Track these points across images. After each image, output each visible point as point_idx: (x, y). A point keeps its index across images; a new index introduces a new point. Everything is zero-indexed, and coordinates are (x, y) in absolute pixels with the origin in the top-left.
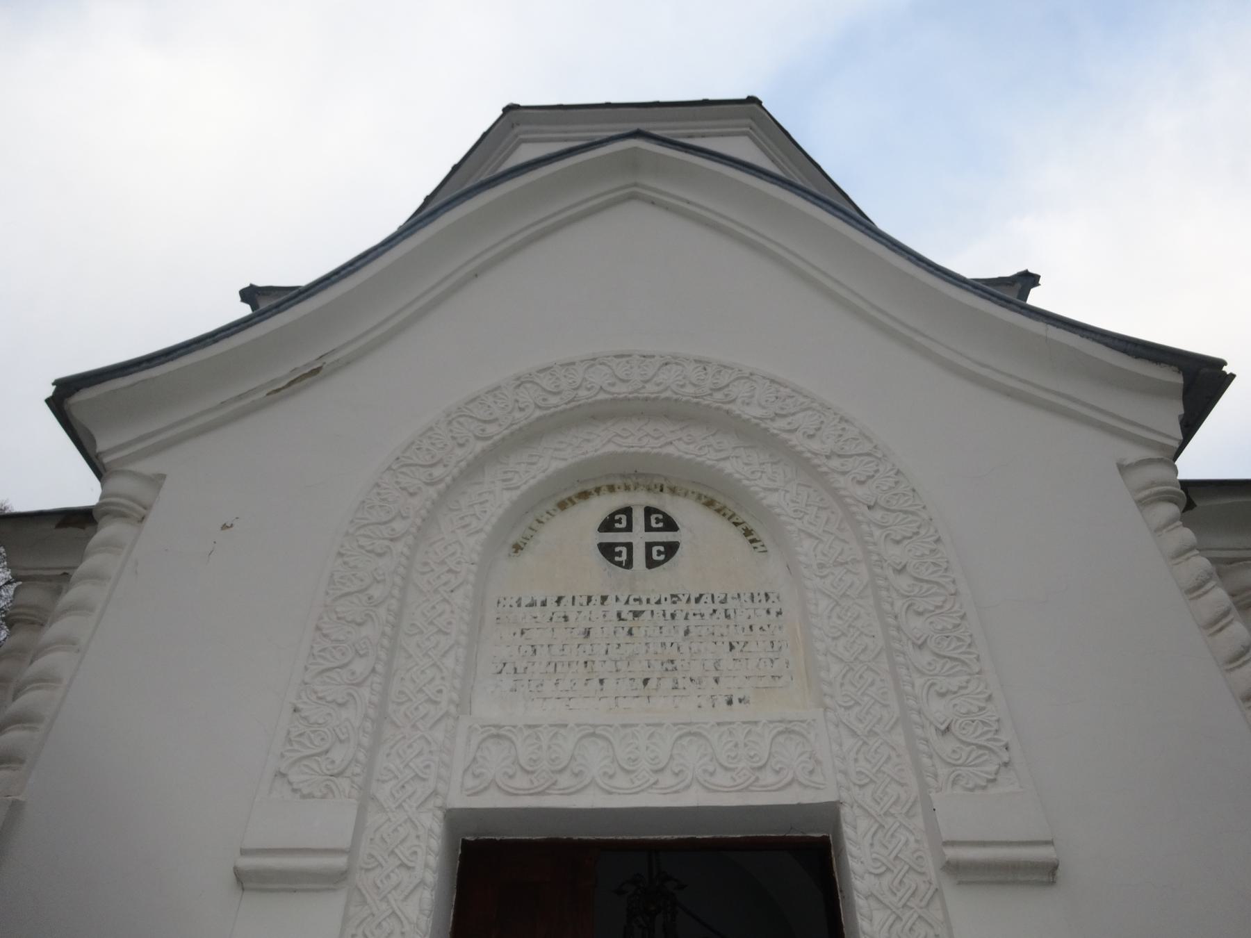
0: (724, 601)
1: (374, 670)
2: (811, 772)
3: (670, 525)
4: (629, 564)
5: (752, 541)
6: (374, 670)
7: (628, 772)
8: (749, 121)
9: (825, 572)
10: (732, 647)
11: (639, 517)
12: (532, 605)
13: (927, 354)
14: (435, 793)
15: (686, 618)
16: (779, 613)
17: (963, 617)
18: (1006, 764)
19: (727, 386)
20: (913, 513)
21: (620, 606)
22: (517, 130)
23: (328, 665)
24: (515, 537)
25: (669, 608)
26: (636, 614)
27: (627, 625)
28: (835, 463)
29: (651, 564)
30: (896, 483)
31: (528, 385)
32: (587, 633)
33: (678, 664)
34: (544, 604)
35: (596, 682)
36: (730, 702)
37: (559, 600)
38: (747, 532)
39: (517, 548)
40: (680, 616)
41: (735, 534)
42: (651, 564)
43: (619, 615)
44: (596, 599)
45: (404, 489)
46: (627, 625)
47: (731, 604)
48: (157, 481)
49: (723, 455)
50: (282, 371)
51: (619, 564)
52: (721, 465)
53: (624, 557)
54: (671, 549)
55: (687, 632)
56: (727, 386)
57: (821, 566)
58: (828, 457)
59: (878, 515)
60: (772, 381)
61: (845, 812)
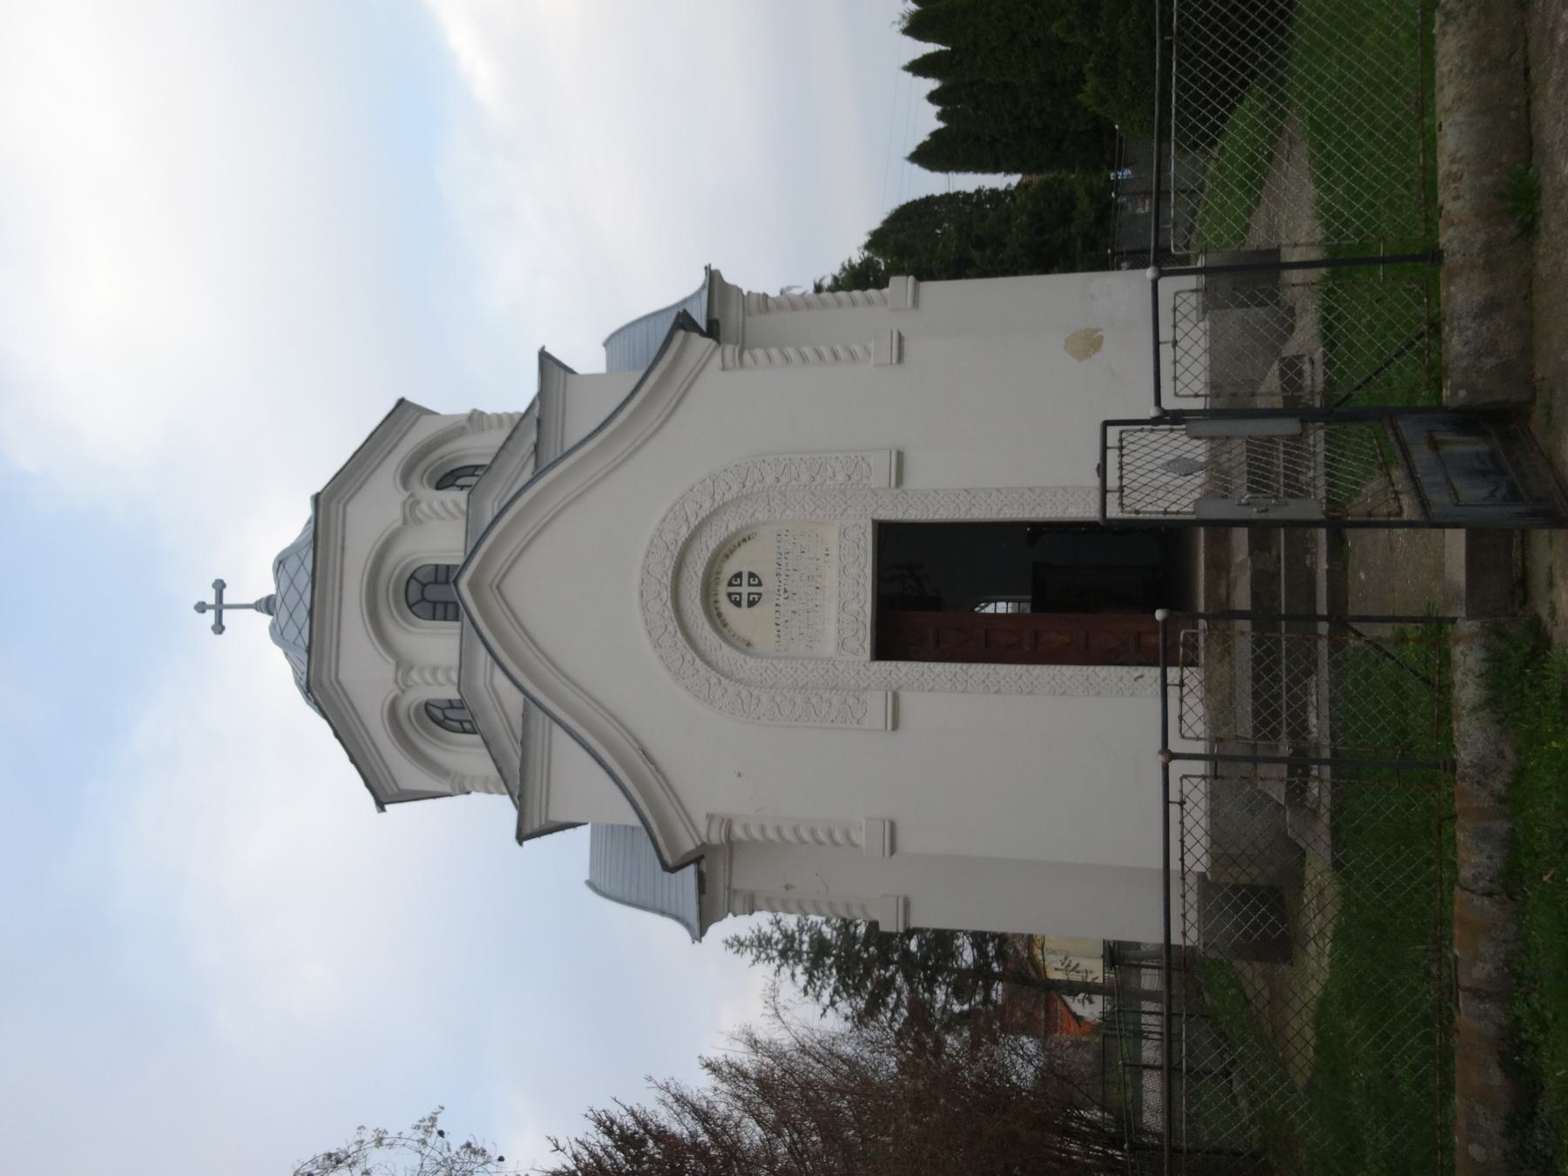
0: (781, 554)
1: (816, 694)
2: (860, 527)
3: (739, 575)
4: (760, 595)
5: (749, 538)
6: (816, 694)
7: (858, 594)
8: (333, 505)
9: (772, 510)
10: (803, 552)
11: (732, 589)
12: (779, 636)
13: (645, 442)
14: (864, 666)
15: (788, 570)
16: (787, 531)
17: (801, 460)
18: (863, 459)
19: (666, 543)
20: (749, 469)
21: (781, 599)
22: (326, 682)
23: (813, 713)
24: (743, 646)
25: (783, 577)
26: (786, 591)
27: (791, 595)
28: (717, 498)
29: (760, 584)
30: (731, 472)
31: (660, 641)
32: (794, 612)
33: (810, 574)
34: (779, 631)
35: (817, 609)
36: (828, 555)
37: (777, 625)
38: (744, 540)
39: (749, 644)
40: (787, 573)
41: (744, 547)
42: (760, 584)
43: (785, 599)
44: (777, 608)
45: (723, 695)
46: (791, 595)
47: (782, 550)
48: (710, 817)
49: (704, 548)
50: (646, 770)
51: (759, 599)
52: (711, 549)
53: (756, 596)
54: (752, 575)
55: (795, 570)
56: (666, 543)
57: (770, 511)
58: (714, 500)
59: (748, 484)
60: (664, 520)
61: (876, 517)
